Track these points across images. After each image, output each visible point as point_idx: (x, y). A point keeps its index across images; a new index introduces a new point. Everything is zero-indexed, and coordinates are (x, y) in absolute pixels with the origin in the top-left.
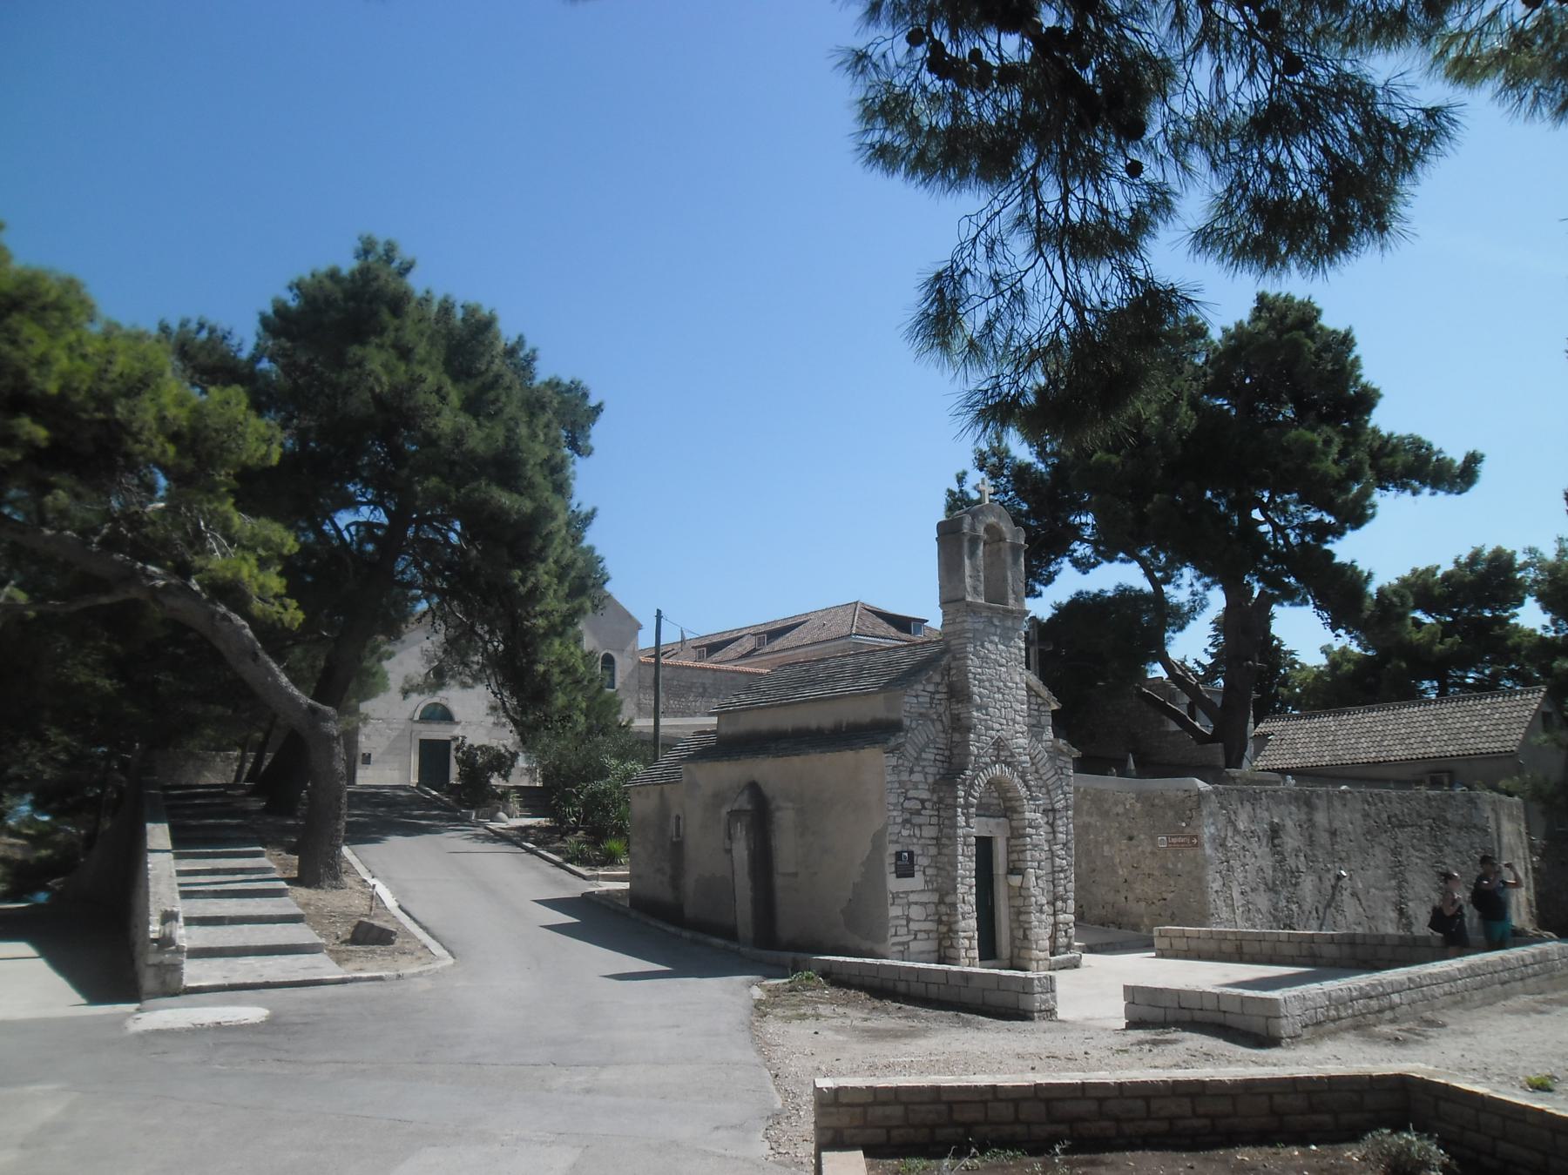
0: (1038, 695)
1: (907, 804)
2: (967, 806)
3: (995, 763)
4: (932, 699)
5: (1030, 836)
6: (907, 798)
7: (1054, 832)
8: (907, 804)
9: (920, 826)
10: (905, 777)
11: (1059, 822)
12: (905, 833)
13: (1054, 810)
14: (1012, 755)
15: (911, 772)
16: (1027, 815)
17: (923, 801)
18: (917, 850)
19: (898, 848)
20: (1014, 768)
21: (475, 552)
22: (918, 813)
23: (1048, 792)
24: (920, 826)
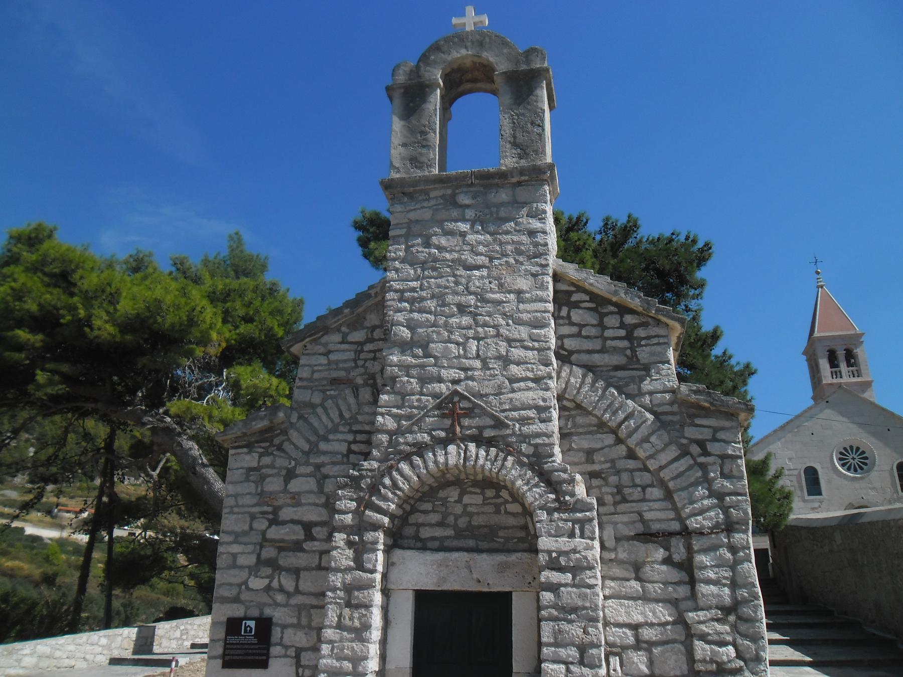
0: (623, 310)
1: (274, 533)
2: (362, 526)
3: (444, 443)
4: (358, 352)
5: (554, 588)
6: (275, 521)
7: (692, 582)
8: (274, 533)
9: (296, 572)
10: (273, 485)
11: (703, 559)
12: (257, 583)
13: (686, 533)
14: (499, 424)
15: (290, 475)
16: (544, 542)
17: (308, 527)
18: (279, 615)
19: (237, 611)
20: (508, 449)
21: (395, 359)
22: (297, 547)
23: (669, 495)
24: (296, 572)
